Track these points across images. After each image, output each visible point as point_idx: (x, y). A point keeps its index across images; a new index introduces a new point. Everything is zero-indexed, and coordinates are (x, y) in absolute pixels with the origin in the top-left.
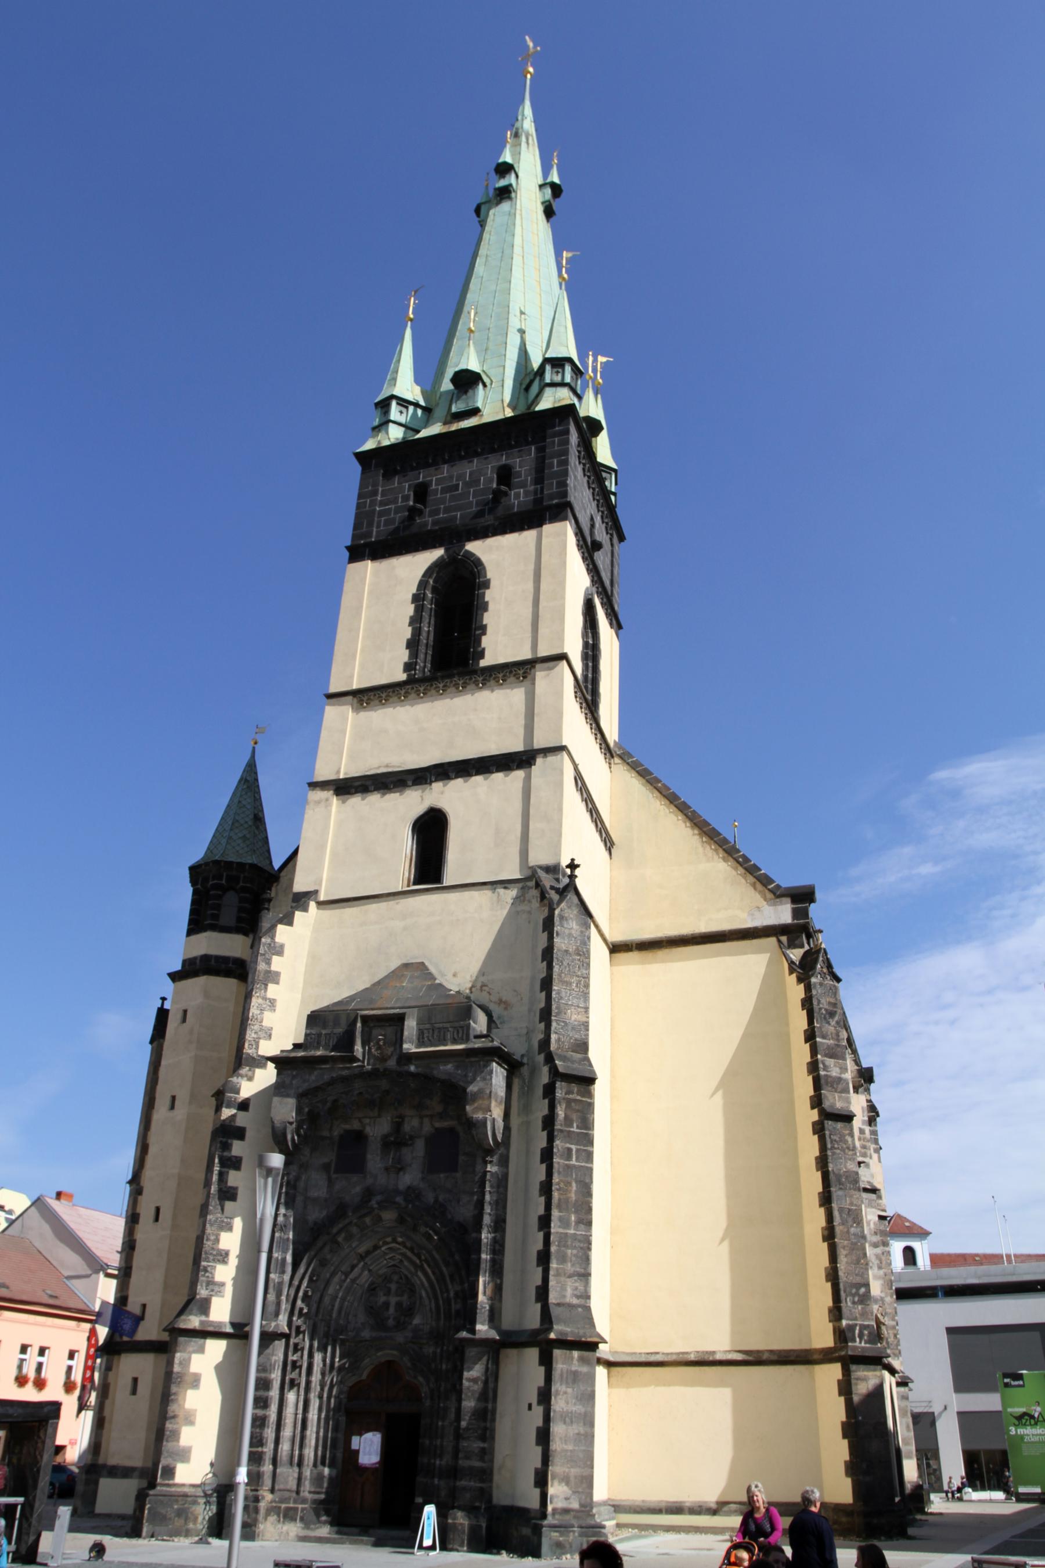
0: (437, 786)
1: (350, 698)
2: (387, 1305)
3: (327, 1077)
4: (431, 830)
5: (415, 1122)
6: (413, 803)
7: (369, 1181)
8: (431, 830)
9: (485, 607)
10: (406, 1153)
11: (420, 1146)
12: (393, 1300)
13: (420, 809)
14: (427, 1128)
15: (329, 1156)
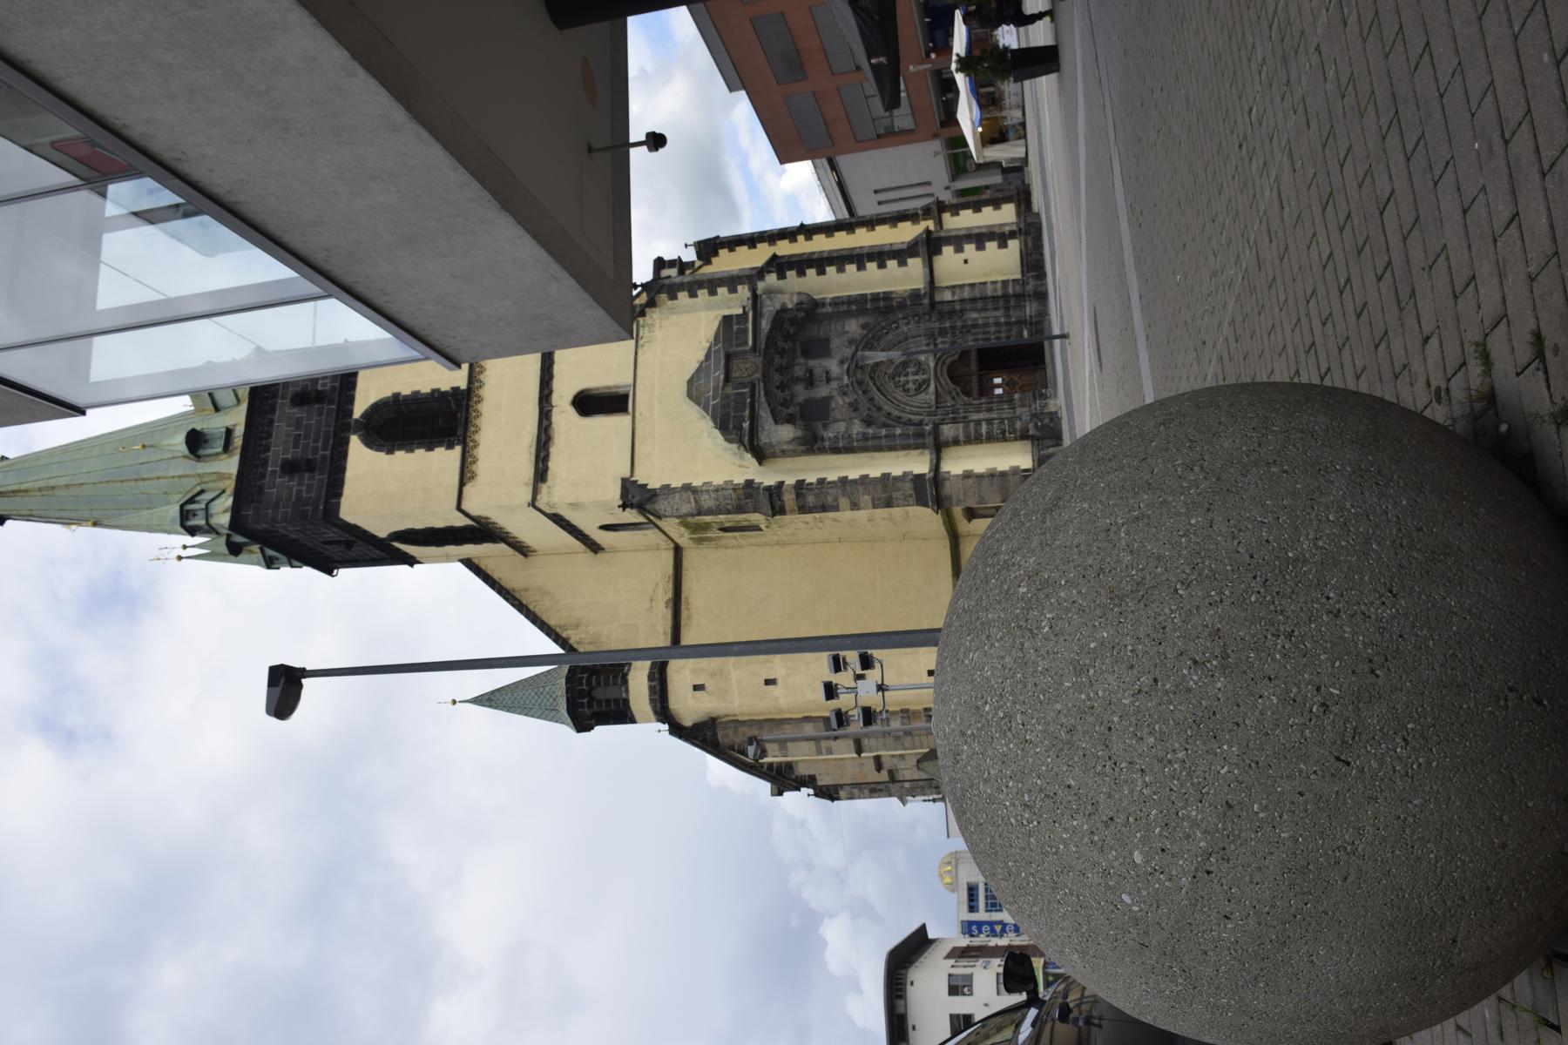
0: (555, 399)
1: (466, 489)
2: (914, 382)
3: (765, 405)
4: (588, 403)
5: (797, 369)
6: (564, 416)
7: (835, 393)
8: (588, 403)
9: (416, 393)
10: (818, 371)
11: (812, 363)
12: (911, 378)
13: (572, 411)
14: (802, 361)
15: (819, 425)
